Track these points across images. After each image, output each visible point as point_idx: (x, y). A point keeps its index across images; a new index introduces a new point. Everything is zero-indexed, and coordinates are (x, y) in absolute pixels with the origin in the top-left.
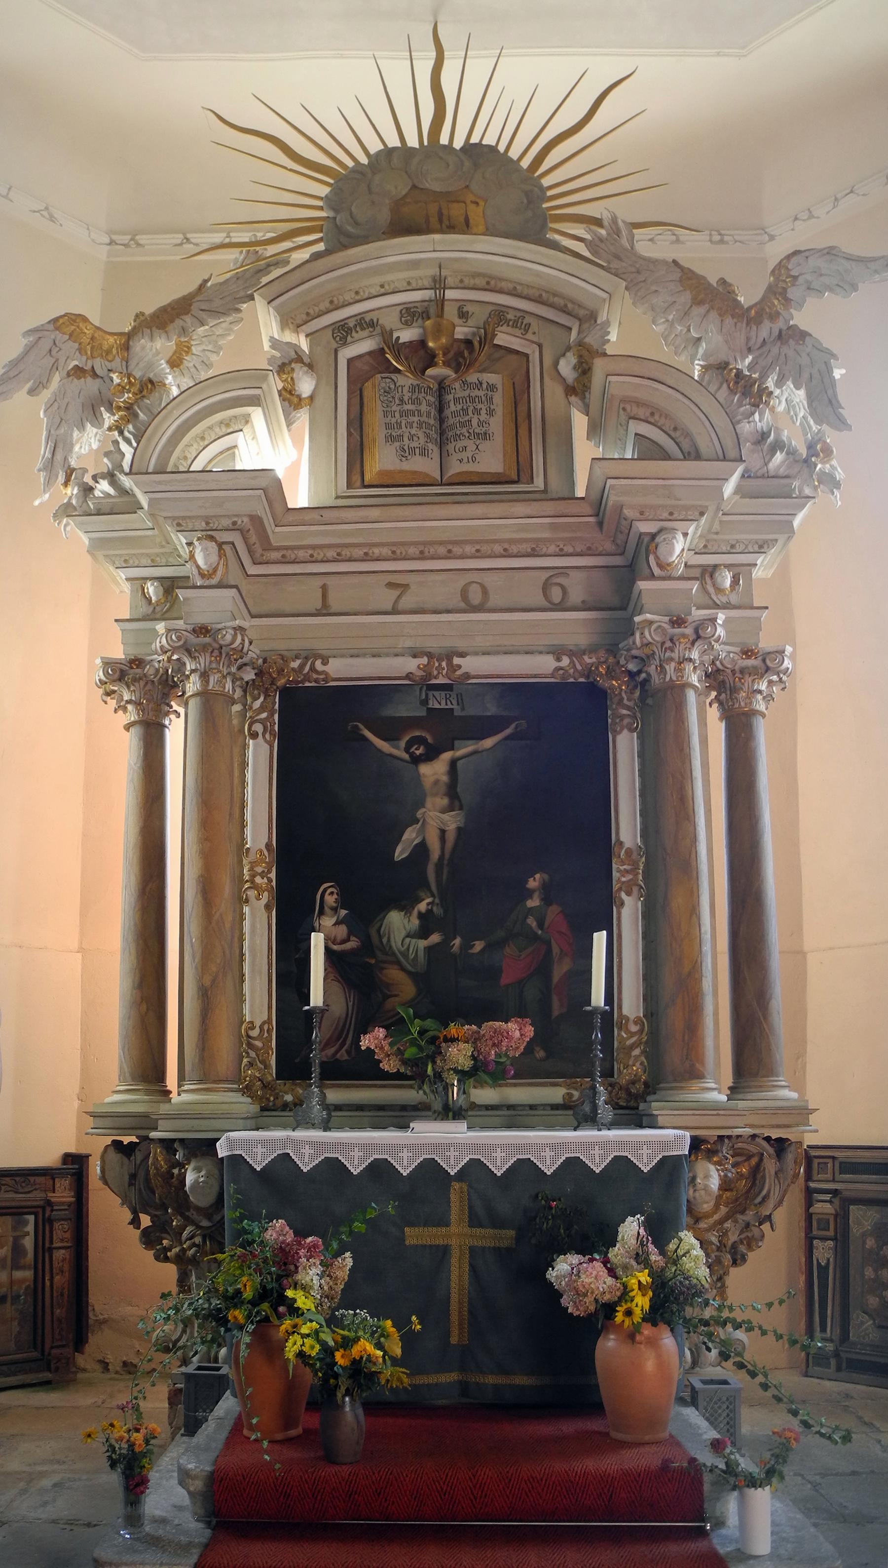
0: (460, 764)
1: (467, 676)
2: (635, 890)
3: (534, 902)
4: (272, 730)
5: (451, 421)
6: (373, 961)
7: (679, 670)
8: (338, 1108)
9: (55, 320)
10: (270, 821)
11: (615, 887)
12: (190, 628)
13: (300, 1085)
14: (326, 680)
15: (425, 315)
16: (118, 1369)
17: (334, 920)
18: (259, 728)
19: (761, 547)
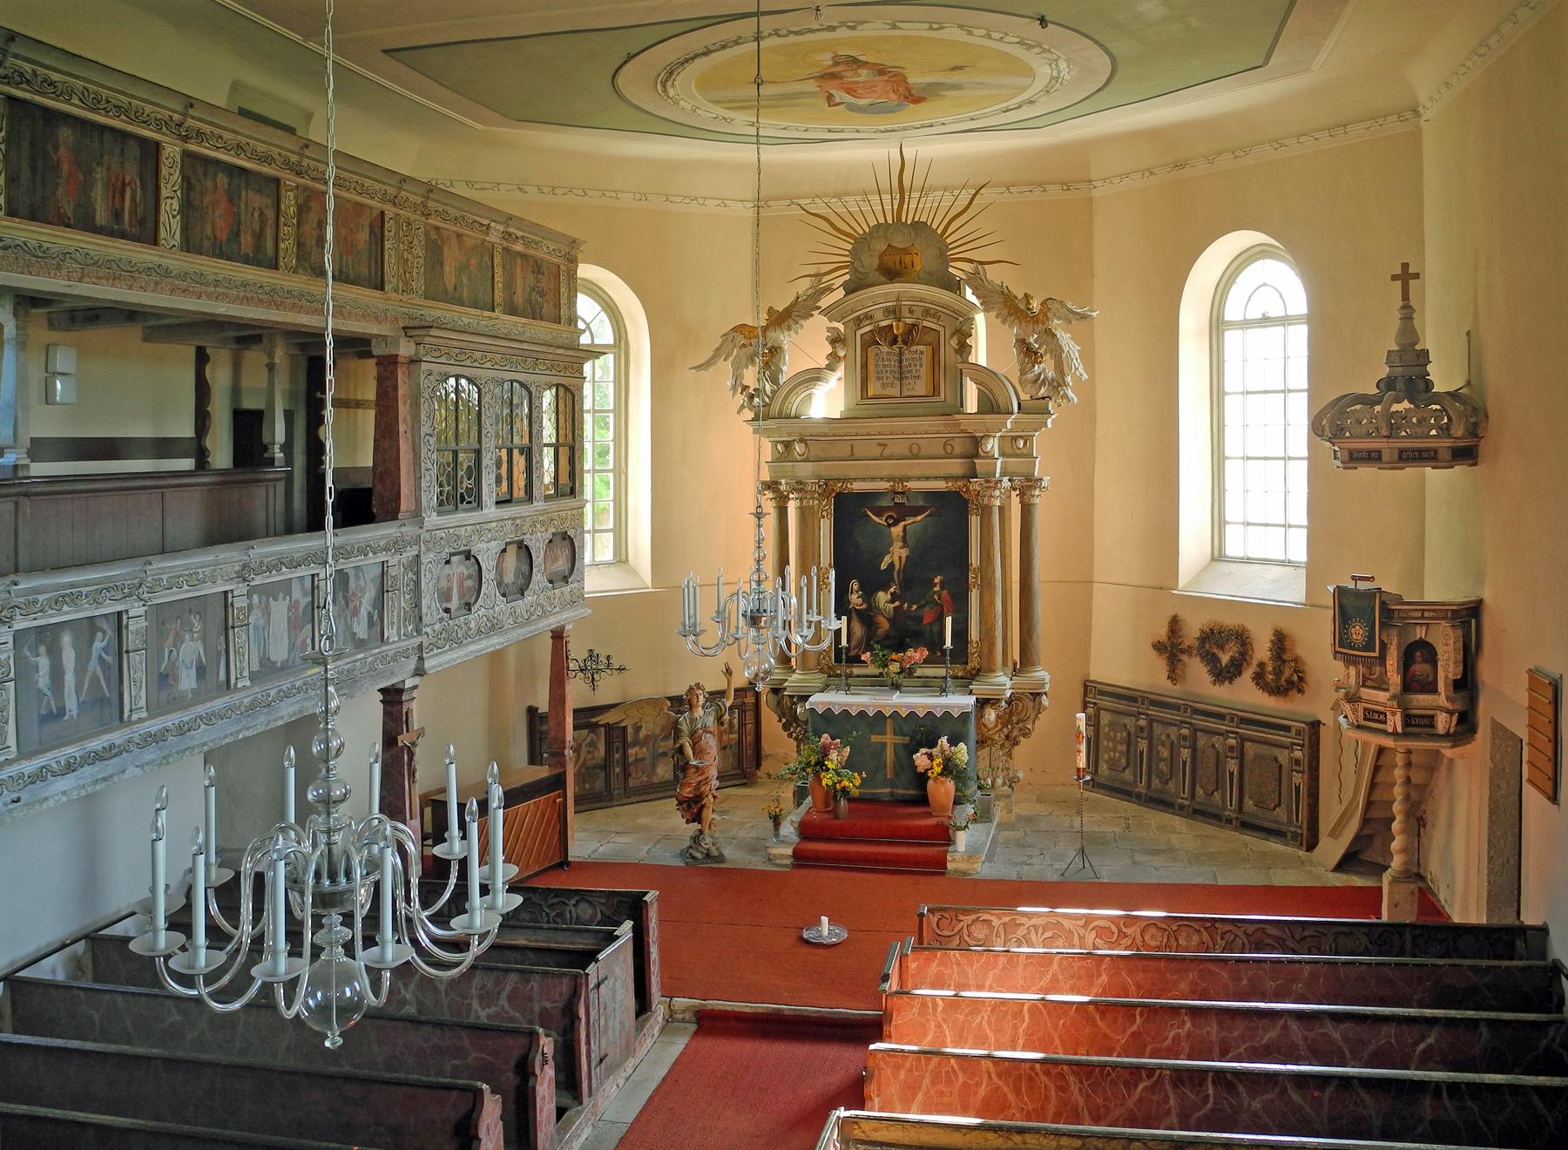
3: (937, 589)
5: (904, 369)
15: (894, 312)
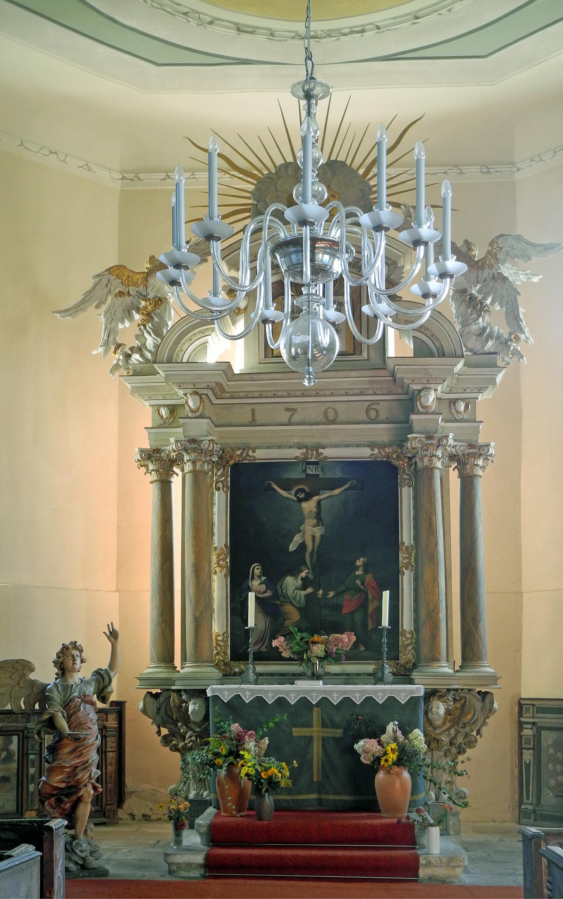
0: (322, 502)
1: (326, 458)
2: (410, 567)
4: (227, 485)
6: (278, 603)
7: (430, 461)
8: (261, 675)
9: (109, 269)
10: (227, 533)
11: (400, 565)
12: (186, 439)
13: (243, 664)
14: (254, 460)
16: (140, 818)
17: (259, 582)
18: (220, 485)
19: (480, 390)
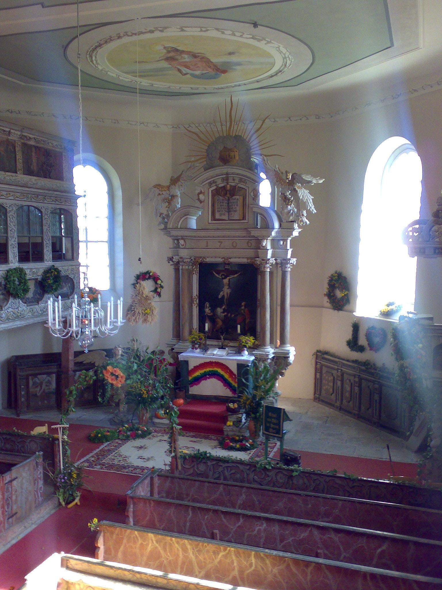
0: (231, 280)
3: (243, 308)
